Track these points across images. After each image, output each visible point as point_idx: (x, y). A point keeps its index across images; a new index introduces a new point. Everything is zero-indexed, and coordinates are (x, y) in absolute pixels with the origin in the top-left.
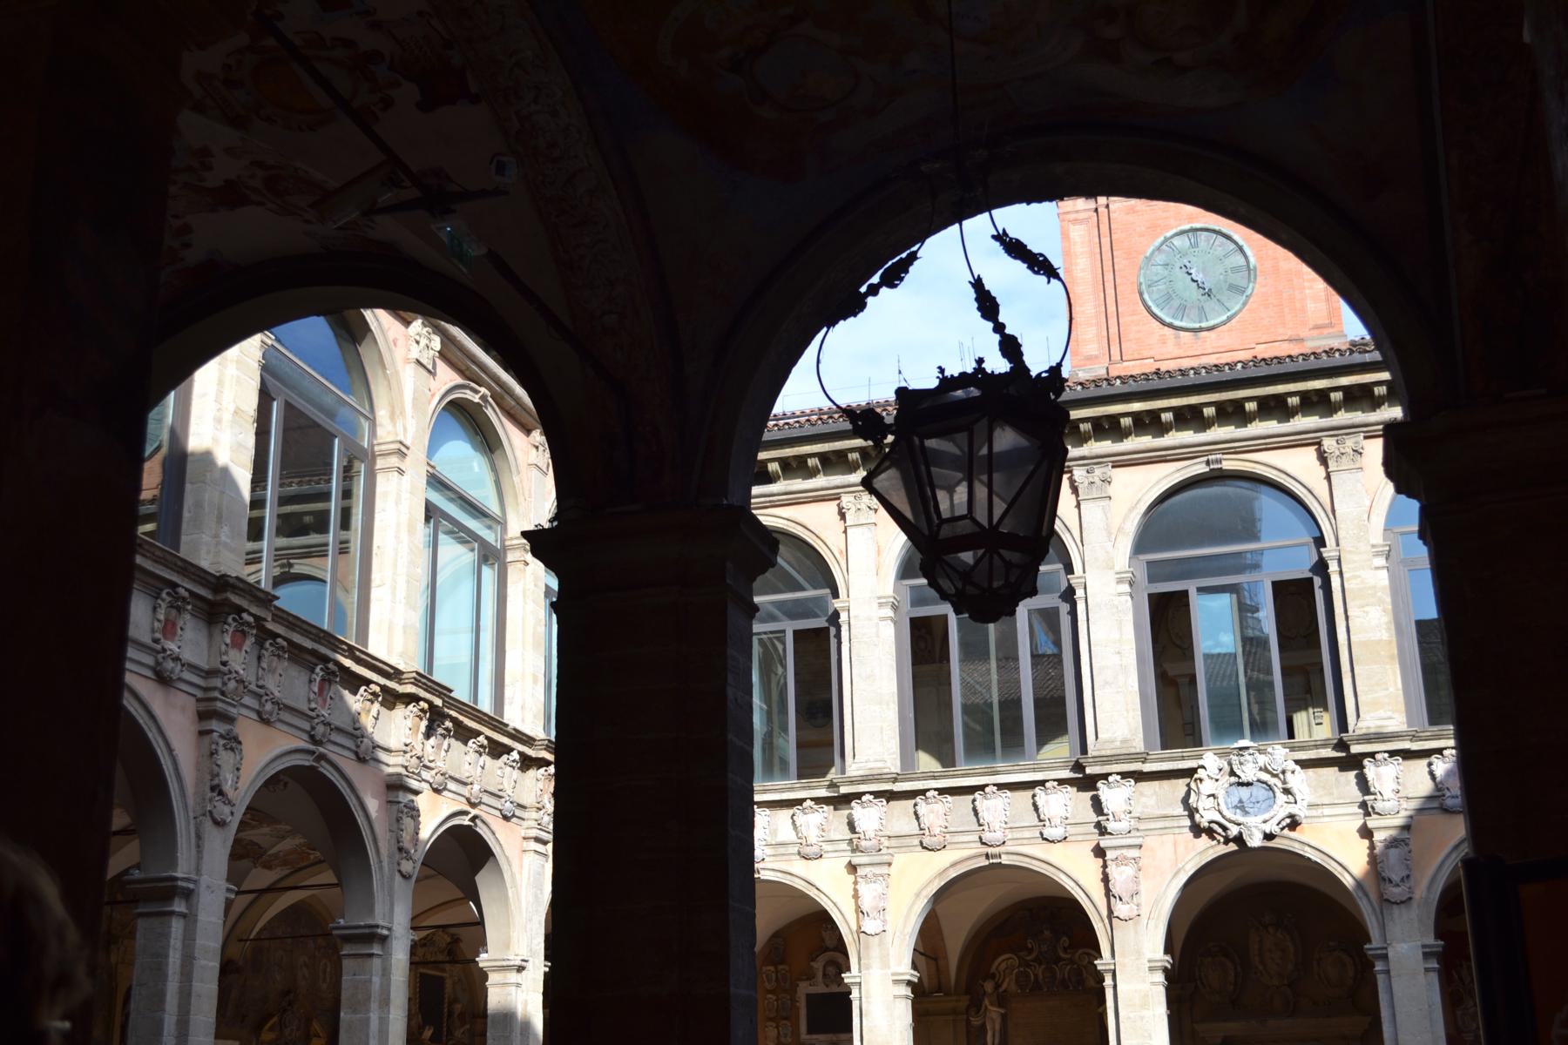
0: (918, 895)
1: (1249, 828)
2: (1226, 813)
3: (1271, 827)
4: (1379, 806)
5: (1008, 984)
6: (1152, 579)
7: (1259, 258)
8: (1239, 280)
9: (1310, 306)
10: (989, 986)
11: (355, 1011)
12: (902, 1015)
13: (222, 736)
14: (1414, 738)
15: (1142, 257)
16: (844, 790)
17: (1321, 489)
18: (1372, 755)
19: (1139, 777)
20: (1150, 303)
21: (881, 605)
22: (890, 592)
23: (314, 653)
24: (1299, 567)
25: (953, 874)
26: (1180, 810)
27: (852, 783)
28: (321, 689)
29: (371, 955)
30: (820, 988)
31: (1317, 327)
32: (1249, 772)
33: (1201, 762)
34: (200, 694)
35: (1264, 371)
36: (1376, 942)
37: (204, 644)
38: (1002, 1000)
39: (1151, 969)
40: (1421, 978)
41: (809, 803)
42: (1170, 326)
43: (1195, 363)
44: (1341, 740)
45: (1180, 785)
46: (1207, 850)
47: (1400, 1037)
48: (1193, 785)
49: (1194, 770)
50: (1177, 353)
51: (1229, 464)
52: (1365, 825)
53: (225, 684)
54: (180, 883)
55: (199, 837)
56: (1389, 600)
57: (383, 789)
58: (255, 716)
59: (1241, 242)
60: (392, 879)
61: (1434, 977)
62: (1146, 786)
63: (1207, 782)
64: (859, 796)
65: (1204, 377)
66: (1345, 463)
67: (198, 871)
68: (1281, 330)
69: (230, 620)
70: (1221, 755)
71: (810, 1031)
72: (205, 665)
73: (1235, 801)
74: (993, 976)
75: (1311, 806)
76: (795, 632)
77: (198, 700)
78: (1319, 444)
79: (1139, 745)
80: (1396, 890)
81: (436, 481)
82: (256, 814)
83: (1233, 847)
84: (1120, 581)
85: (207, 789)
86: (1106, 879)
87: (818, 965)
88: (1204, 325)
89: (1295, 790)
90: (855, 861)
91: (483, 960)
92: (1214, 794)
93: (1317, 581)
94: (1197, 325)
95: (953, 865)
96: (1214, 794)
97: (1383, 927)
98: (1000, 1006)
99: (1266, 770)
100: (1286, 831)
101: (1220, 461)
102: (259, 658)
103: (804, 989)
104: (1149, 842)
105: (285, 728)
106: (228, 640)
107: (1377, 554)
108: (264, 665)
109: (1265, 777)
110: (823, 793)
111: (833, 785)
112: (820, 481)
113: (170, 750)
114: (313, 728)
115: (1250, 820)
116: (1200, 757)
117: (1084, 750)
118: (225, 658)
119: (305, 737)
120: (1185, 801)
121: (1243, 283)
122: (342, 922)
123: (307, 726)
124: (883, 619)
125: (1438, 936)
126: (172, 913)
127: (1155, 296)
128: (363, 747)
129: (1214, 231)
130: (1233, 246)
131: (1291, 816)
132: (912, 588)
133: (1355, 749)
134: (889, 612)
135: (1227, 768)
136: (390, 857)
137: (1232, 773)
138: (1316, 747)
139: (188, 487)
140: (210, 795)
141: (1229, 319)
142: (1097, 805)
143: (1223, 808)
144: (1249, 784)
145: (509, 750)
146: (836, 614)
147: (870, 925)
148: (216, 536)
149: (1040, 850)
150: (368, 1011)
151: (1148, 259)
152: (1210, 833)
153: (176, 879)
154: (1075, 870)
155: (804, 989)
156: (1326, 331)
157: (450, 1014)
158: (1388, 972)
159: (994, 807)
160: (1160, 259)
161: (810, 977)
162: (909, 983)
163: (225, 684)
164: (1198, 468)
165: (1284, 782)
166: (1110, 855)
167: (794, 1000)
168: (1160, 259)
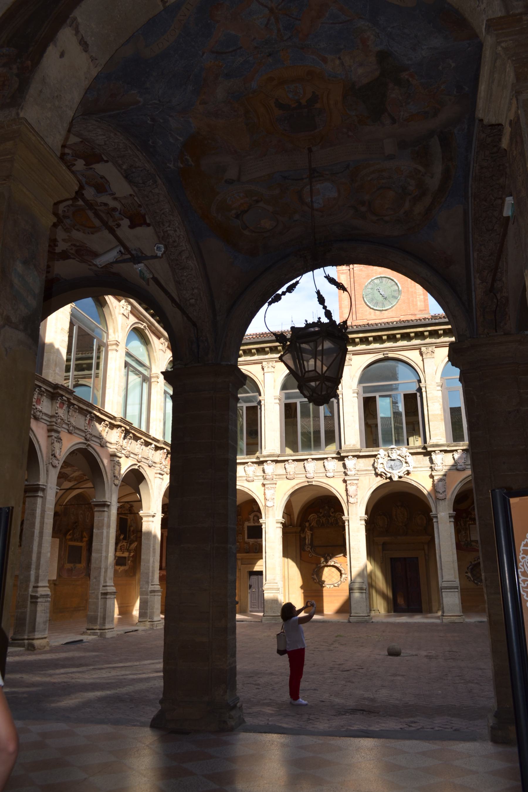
0: (285, 494)
1: (393, 474)
2: (386, 469)
3: (401, 474)
4: (436, 468)
5: (314, 524)
6: (364, 392)
7: (402, 287)
8: (396, 294)
9: (419, 303)
10: (307, 524)
11: (98, 529)
12: (279, 533)
13: (55, 438)
14: (448, 446)
15: (364, 286)
16: (261, 459)
17: (420, 364)
18: (434, 451)
19: (358, 457)
20: (366, 301)
21: (275, 399)
22: (278, 394)
23: (87, 410)
24: (412, 390)
25: (297, 487)
26: (371, 468)
27: (264, 457)
28: (89, 422)
29: (104, 511)
30: (252, 524)
31: (421, 311)
32: (394, 456)
33: (379, 453)
34: (48, 423)
35: (403, 325)
36: (434, 512)
37: (50, 406)
38: (311, 529)
39: (361, 520)
40: (448, 524)
42: (373, 309)
43: (380, 321)
44: (424, 446)
45: (372, 460)
46: (380, 481)
47: (441, 543)
48: (376, 460)
49: (376, 455)
50: (374, 317)
51: (391, 355)
52: (431, 474)
53: (57, 420)
54: (41, 486)
55: (47, 471)
56: (441, 401)
57: (109, 456)
58: (66, 431)
59: (397, 282)
60: (112, 486)
61: (452, 524)
62: (361, 460)
63: (380, 459)
64: (266, 461)
65: (383, 326)
66: (429, 356)
67: (47, 482)
68: (409, 311)
69: (59, 399)
70: (385, 450)
71: (248, 538)
72: (50, 413)
73: (389, 465)
74: (309, 521)
75: (414, 467)
76: (247, 407)
77: (48, 425)
78: (420, 349)
79: (358, 447)
80: (441, 495)
81: (128, 354)
82: (66, 464)
83: (388, 480)
84: (354, 393)
85: (50, 455)
86: (347, 490)
87: (251, 516)
88: (384, 309)
89: (409, 462)
90: (265, 483)
91: (141, 513)
92: (383, 463)
93: (418, 394)
94: (381, 309)
95: (297, 484)
96: (383, 463)
97: (436, 507)
98: (311, 531)
99: (400, 455)
100: (406, 476)
101: (387, 354)
102: (68, 412)
103: (247, 524)
104: (361, 478)
105: (76, 435)
106: (58, 406)
107: (438, 386)
108: (70, 414)
109: (400, 458)
110: (255, 460)
111: (258, 458)
112: (256, 357)
113: (38, 442)
114: (86, 436)
115: (394, 472)
116: (378, 451)
117: (341, 448)
118: (57, 412)
119: (83, 438)
120: (373, 465)
121: (397, 295)
122: (94, 500)
123: (84, 435)
124: (276, 403)
125: (454, 510)
126: (38, 496)
127: (368, 299)
128: (103, 442)
129: (388, 278)
130: (394, 283)
131: (408, 471)
132: (285, 393)
133: (429, 449)
134: (278, 401)
135: (387, 455)
136: (111, 479)
137: (389, 456)
138: (416, 448)
139: (45, 354)
140: (51, 457)
141: (392, 307)
142: (344, 466)
144: (394, 460)
145: (151, 444)
146: (260, 402)
147: (269, 504)
148: (54, 371)
149: (325, 480)
150: (103, 529)
151: (366, 286)
152: (381, 476)
153: (39, 485)
154: (337, 487)
155: (247, 524)
156: (423, 312)
157: (129, 530)
158: (437, 522)
159: (311, 466)
160: (370, 286)
161: (248, 520)
162: (281, 523)
163: (57, 420)
164: (380, 356)
165: (406, 460)
166: (348, 482)
167: (243, 528)
168: (370, 286)
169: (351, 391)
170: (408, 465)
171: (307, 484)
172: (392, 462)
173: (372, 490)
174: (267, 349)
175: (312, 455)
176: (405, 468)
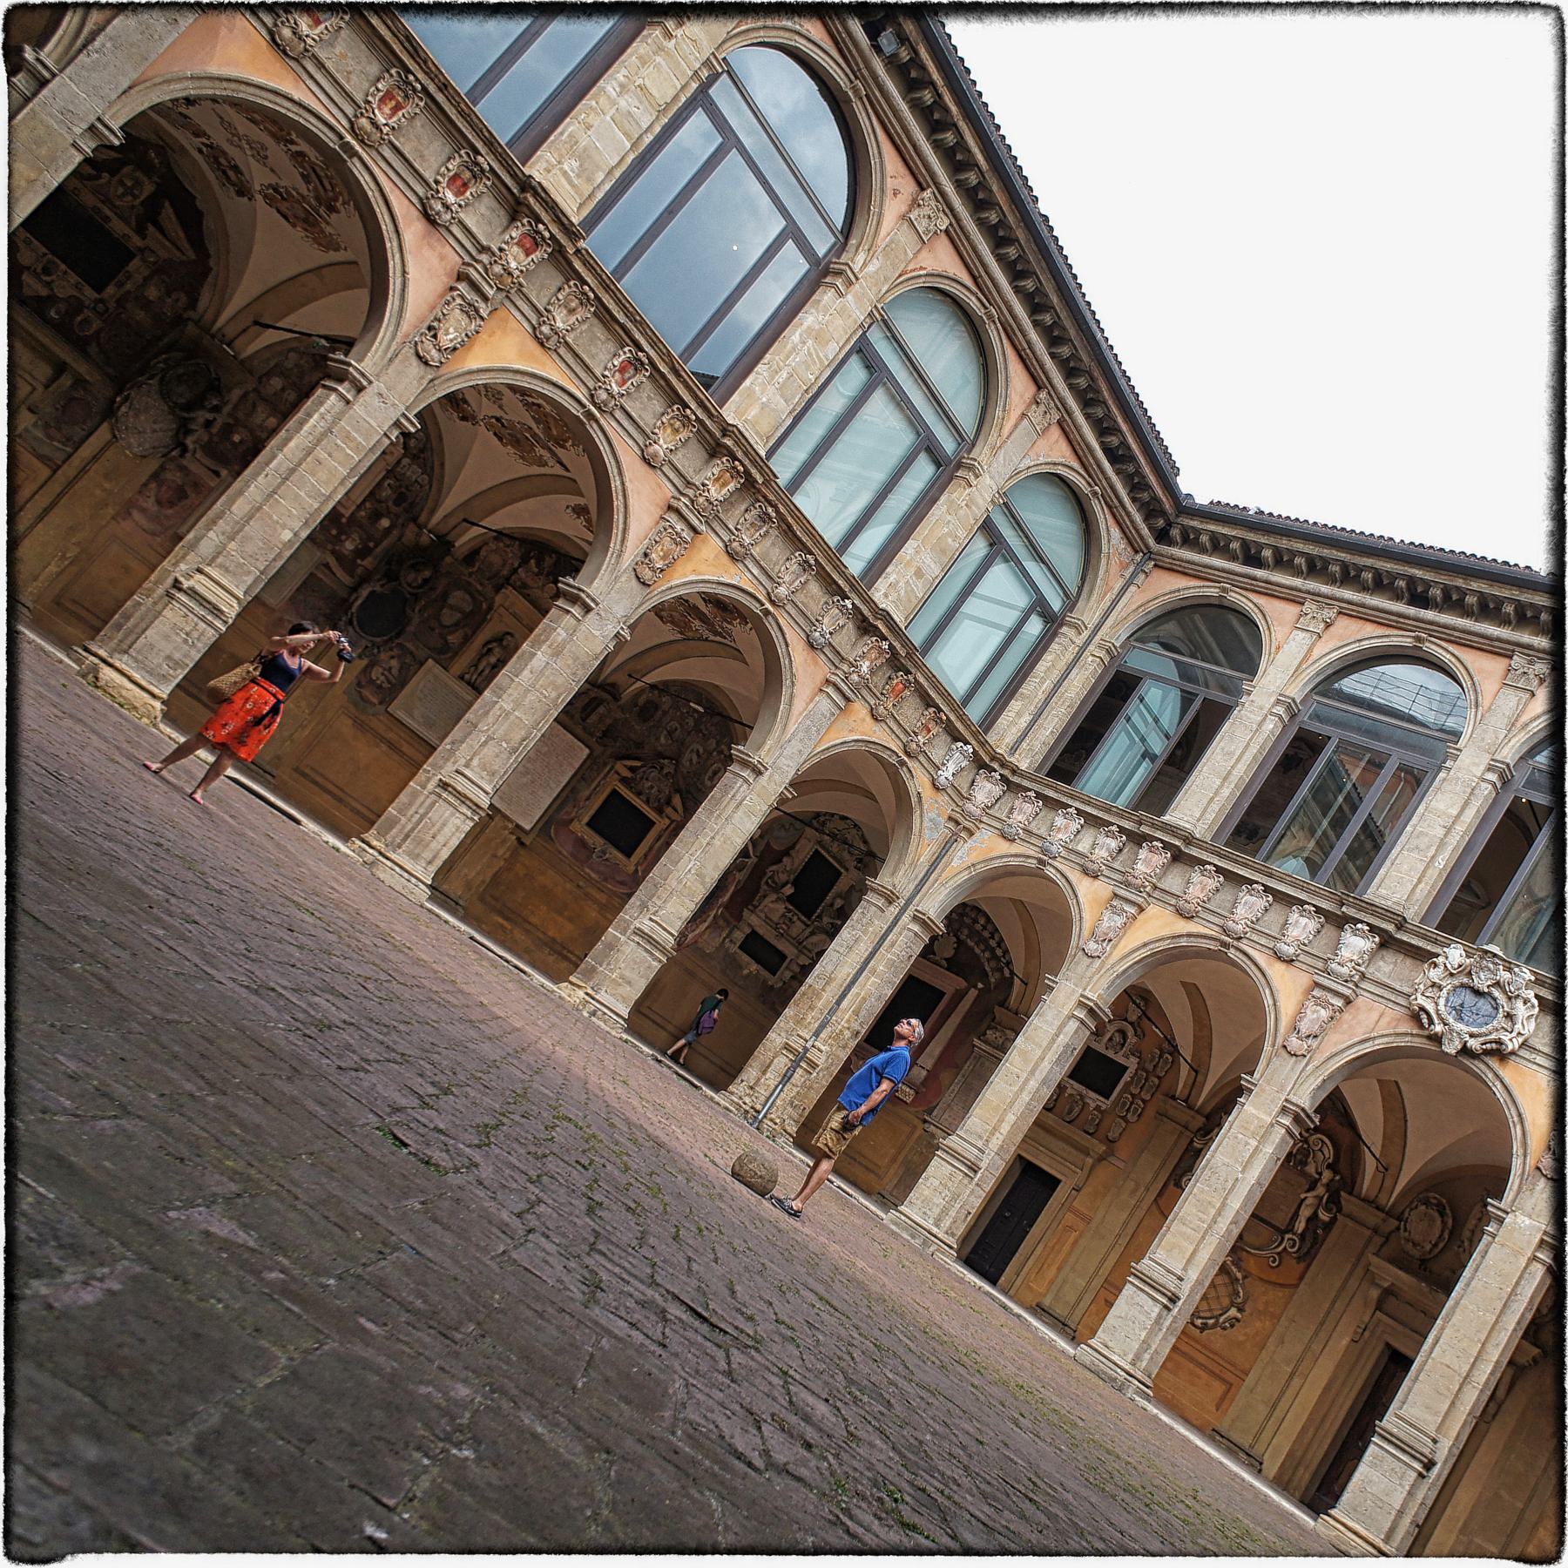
0: (1145, 945)
2: (1442, 1007)
3: (1473, 1044)
25: (1183, 942)
32: (1482, 981)
39: (1284, 1110)
41: (1114, 828)
57: (664, 505)
73: (1457, 1001)
85: (426, 325)
91: (737, 750)
95: (1189, 935)
128: (651, 450)
131: (1499, 1042)
143: (1442, 1002)
144: (1478, 993)
169: (1485, 760)
170: (1508, 1026)
171: (1213, 946)
172: (1469, 998)
173: (1368, 1048)
174: (1335, 568)
175: (1270, 876)
176: (1495, 1029)
